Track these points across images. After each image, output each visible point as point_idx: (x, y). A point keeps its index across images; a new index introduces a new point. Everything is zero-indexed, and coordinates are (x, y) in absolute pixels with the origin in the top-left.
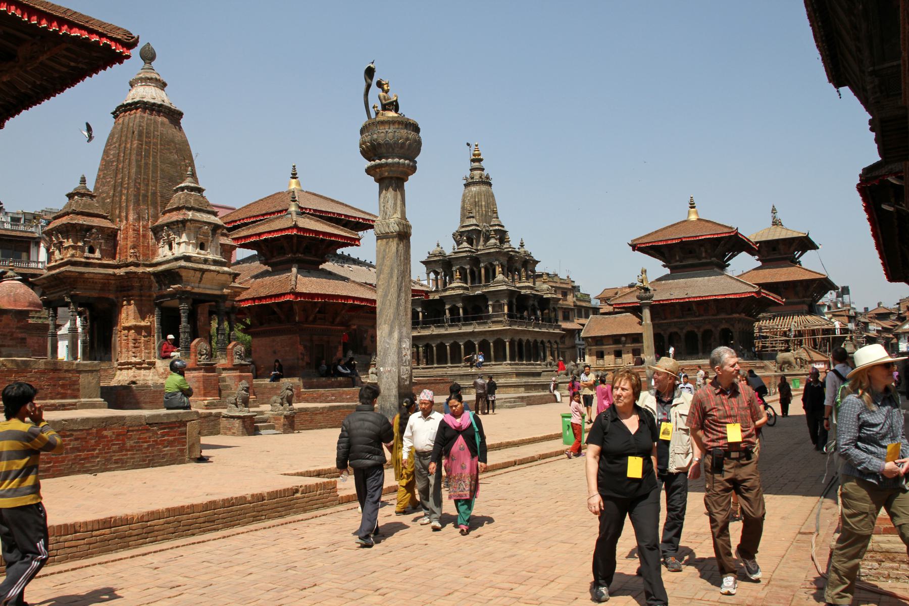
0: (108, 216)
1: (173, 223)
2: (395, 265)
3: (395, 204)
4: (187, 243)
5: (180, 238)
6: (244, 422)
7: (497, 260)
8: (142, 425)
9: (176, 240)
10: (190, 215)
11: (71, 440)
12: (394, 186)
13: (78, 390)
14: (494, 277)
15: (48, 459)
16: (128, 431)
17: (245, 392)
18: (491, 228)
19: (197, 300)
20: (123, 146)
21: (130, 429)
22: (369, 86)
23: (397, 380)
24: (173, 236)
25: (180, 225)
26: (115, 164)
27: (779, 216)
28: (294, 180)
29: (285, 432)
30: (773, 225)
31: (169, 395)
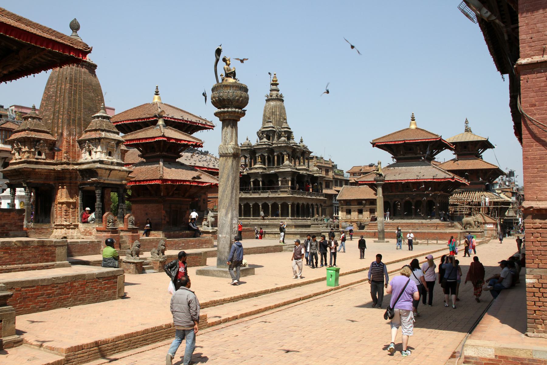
0: (50, 132)
1: (92, 139)
2: (231, 174)
3: (232, 136)
4: (101, 152)
5: (97, 148)
6: (136, 266)
7: (285, 151)
8: (94, 279)
9: (94, 150)
10: (103, 134)
11: (57, 289)
12: (231, 125)
13: (55, 257)
14: (283, 162)
15: (44, 300)
16: (87, 283)
17: (137, 248)
19: (106, 188)
20: (59, 86)
21: (88, 281)
22: (217, 61)
23: (229, 243)
24: (92, 147)
25: (97, 141)
26: (54, 98)
27: (469, 125)
28: (157, 96)
29: (160, 271)
30: (466, 131)
31: (107, 259)
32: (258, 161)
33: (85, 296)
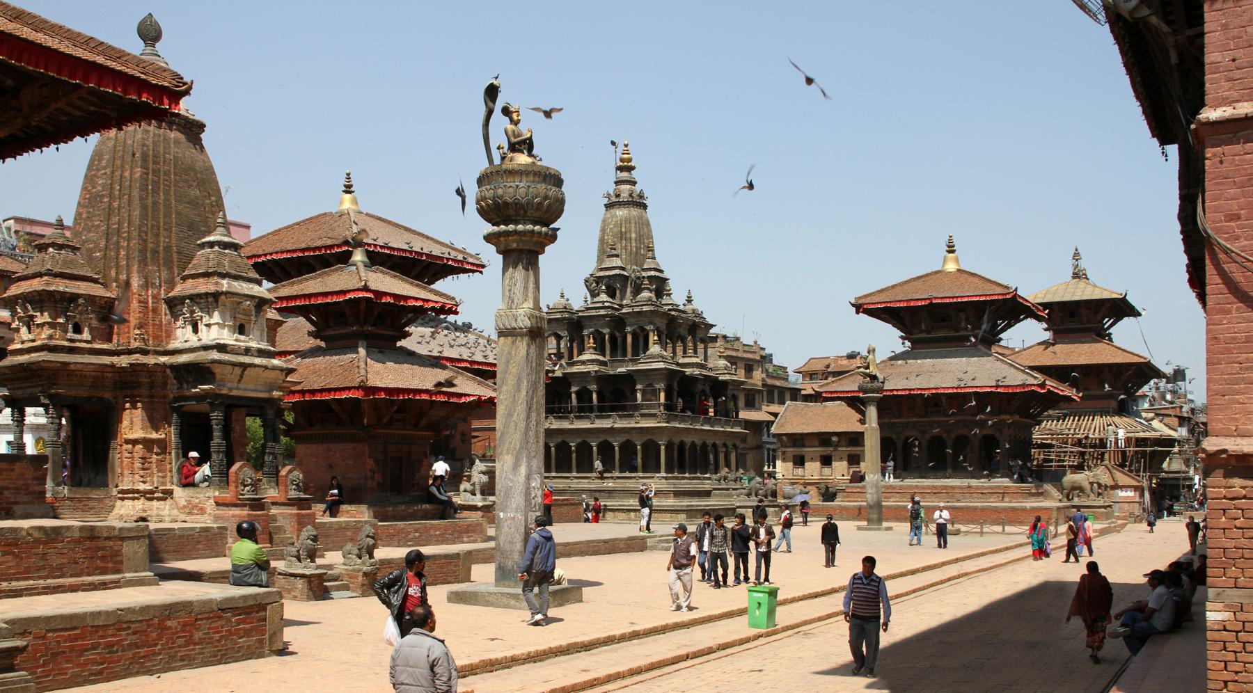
0: (99, 279)
1: (199, 296)
2: (524, 374)
3: (526, 288)
4: (221, 326)
5: (211, 317)
7: (651, 323)
8: (213, 611)
9: (204, 320)
10: (225, 284)
11: (128, 634)
12: (525, 262)
13: (121, 562)
14: (646, 347)
15: (101, 658)
16: (197, 620)
18: (644, 274)
19: (234, 407)
20: (118, 173)
21: (199, 617)
22: (490, 113)
23: (523, 530)
24: (200, 314)
25: (210, 299)
26: (106, 200)
28: (348, 196)
31: (242, 568)
32: (587, 346)
33: (194, 650)
